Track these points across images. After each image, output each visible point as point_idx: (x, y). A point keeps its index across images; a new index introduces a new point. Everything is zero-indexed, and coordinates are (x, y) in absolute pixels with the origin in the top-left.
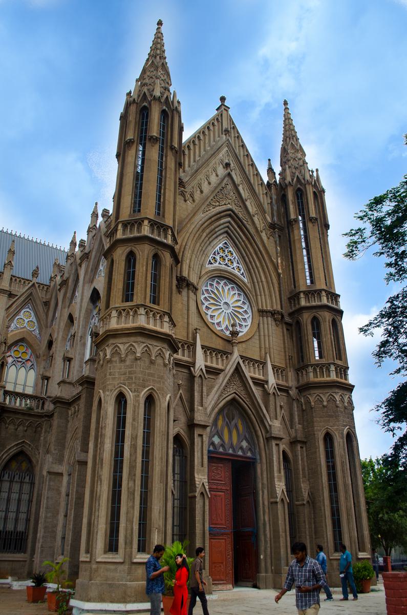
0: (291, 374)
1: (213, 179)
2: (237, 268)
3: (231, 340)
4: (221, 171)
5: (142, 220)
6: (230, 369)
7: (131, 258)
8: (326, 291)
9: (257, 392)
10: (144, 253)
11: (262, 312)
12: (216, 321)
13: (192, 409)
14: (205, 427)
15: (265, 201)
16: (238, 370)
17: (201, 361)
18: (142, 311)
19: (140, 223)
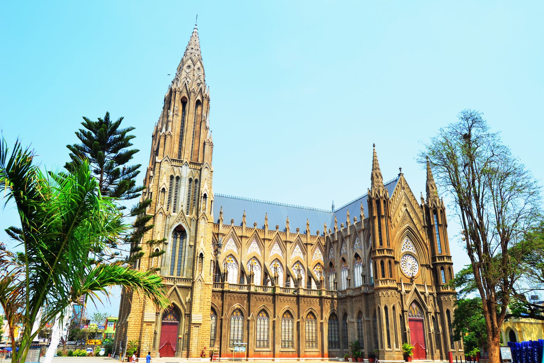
0: (434, 288)
1: (401, 214)
2: (412, 250)
3: (412, 279)
4: (404, 209)
5: (384, 249)
6: (413, 290)
7: (382, 263)
8: (447, 257)
9: (422, 297)
10: (386, 261)
11: (422, 265)
12: (406, 272)
13: (403, 305)
14: (407, 311)
15: (420, 215)
16: (416, 290)
17: (404, 289)
18: (388, 281)
19: (383, 250)
